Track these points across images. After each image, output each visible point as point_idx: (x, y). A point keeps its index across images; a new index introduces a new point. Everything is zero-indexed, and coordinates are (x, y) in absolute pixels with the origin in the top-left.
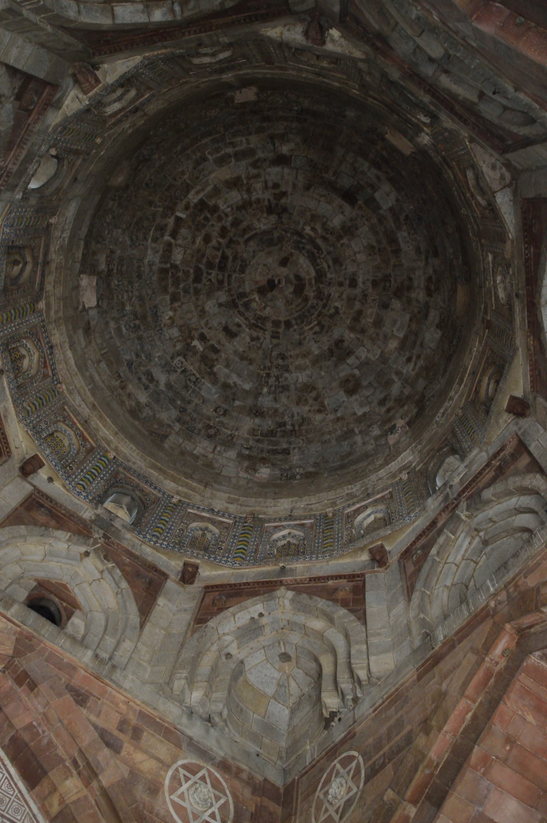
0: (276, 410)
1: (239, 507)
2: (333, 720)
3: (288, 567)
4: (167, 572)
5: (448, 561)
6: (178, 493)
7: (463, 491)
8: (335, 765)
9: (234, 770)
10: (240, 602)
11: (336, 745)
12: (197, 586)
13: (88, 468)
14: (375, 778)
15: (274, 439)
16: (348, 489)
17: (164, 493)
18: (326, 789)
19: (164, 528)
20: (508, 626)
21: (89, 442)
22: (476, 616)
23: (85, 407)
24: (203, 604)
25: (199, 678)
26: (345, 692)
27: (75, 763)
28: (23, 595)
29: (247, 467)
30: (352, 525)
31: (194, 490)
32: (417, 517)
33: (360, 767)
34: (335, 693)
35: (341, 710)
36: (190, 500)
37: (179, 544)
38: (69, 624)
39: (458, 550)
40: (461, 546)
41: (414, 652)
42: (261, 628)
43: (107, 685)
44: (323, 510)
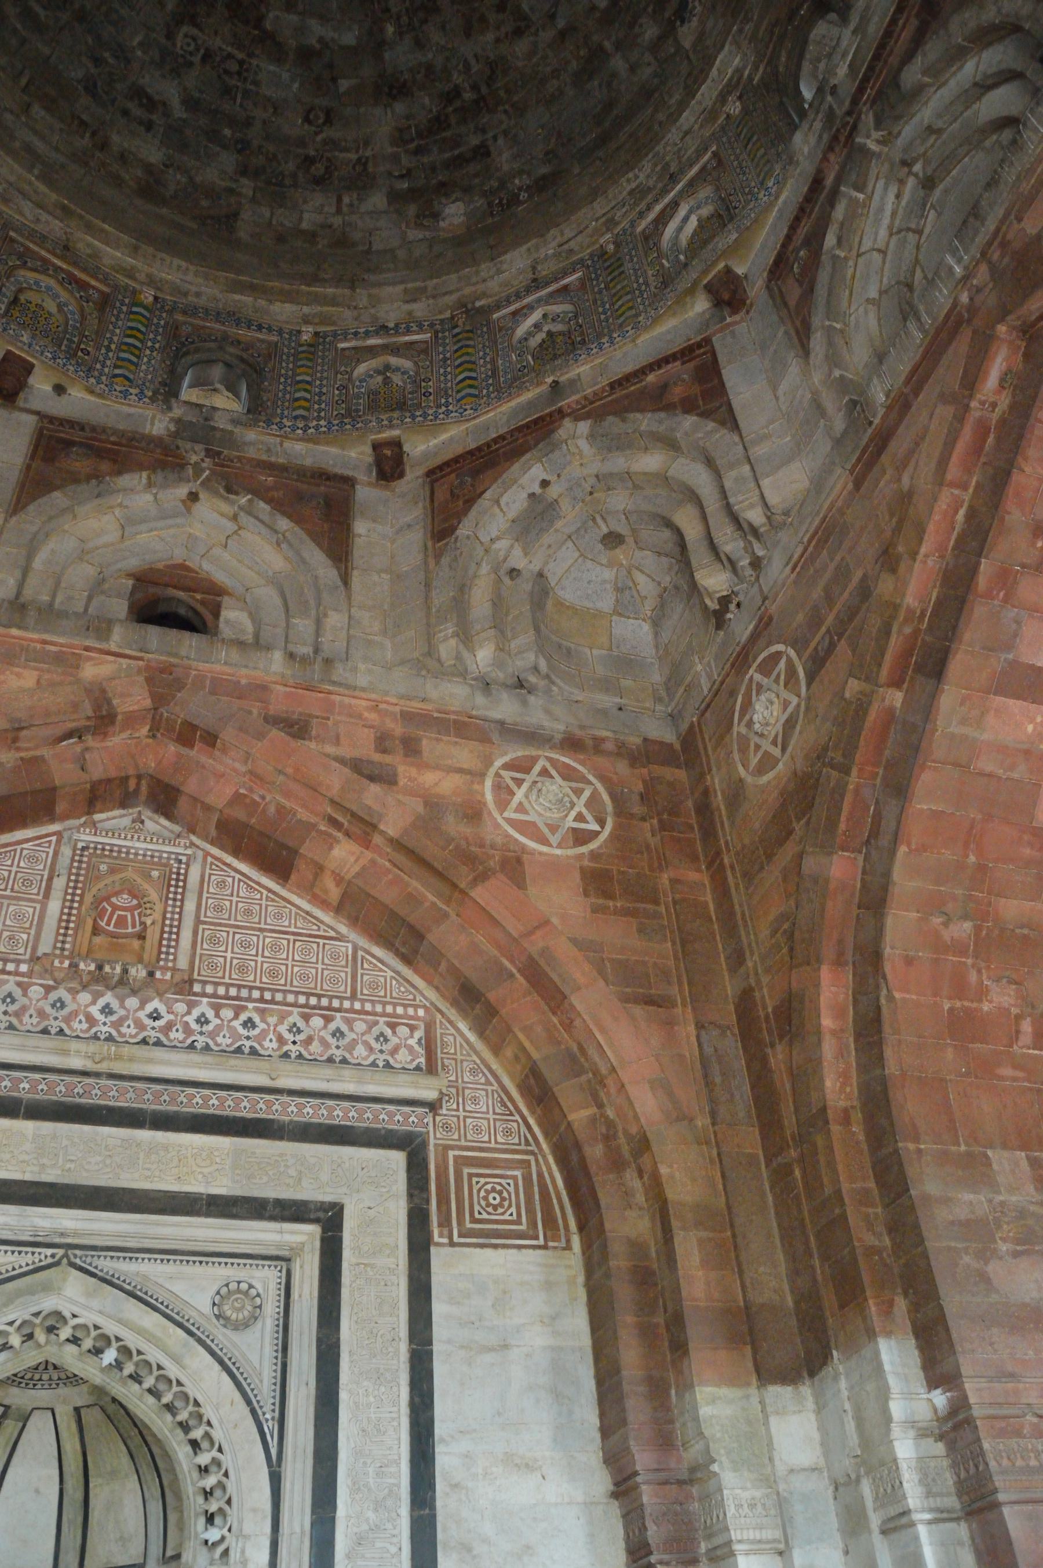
0: (429, 68)
1: (431, 301)
2: (727, 611)
3: (562, 379)
4: (350, 473)
5: (862, 250)
6: (306, 320)
7: (861, 90)
9: (589, 743)
10: (500, 475)
11: (743, 648)
12: (413, 477)
13: (115, 339)
15: (447, 134)
16: (628, 181)
17: (280, 332)
18: (747, 717)
19: (308, 396)
20: (1002, 329)
21: (94, 288)
22: (938, 331)
23: (50, 218)
24: (436, 504)
25: (478, 627)
26: (733, 557)
27: (333, 822)
28: (120, 608)
29: (418, 216)
30: (659, 250)
31: (333, 302)
32: (780, 184)
34: (719, 566)
36: (334, 324)
37: (349, 416)
38: (222, 625)
39: (878, 221)
40: (881, 210)
41: (838, 442)
42: (554, 505)
43: (330, 693)
44: (594, 243)
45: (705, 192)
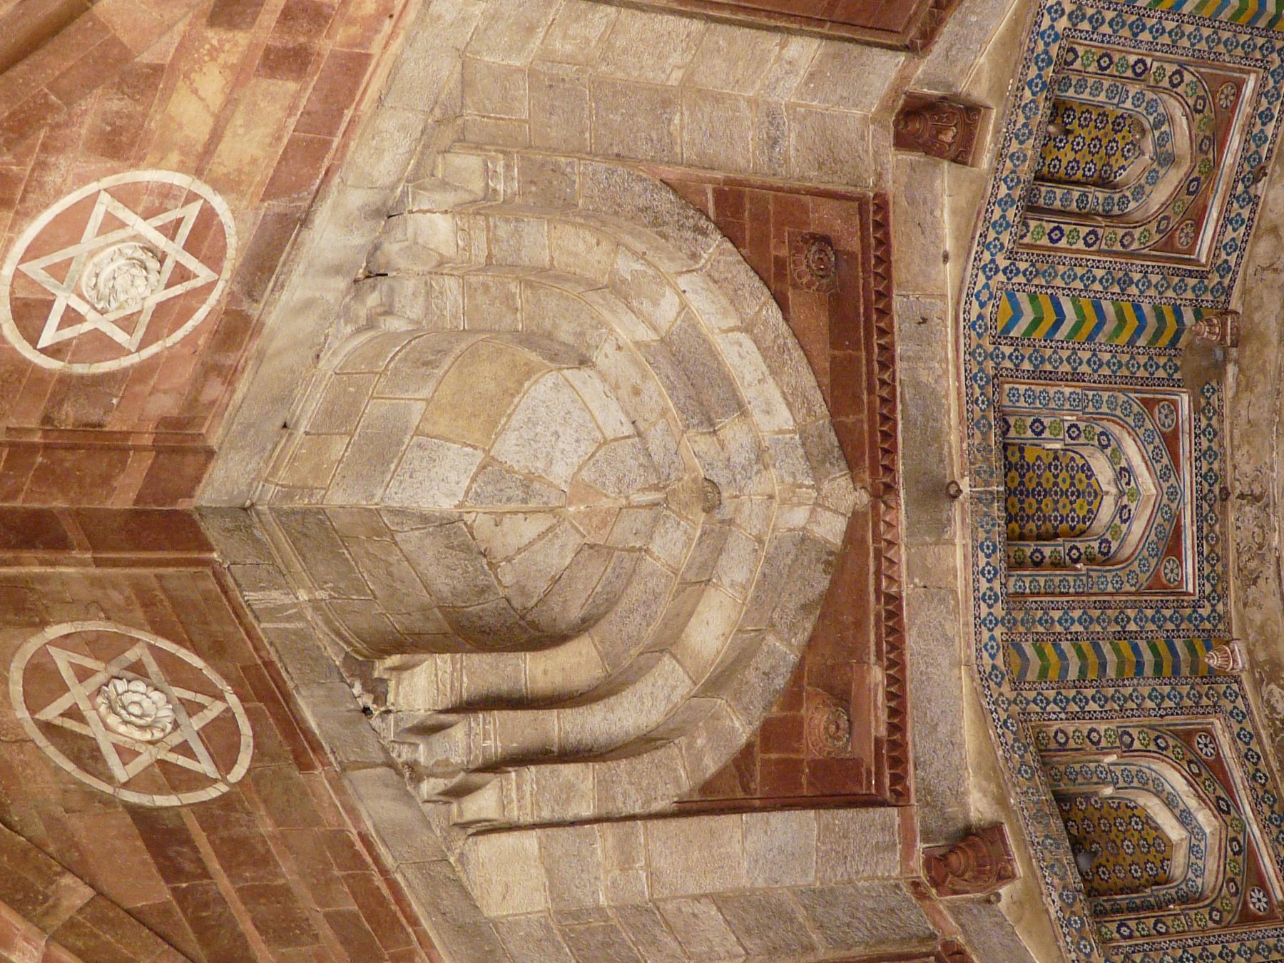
2: (368, 688)
3: (956, 511)
4: (938, 48)
8: (220, 697)
9: (230, 359)
14: (139, 843)
25: (503, 230)
33: (189, 789)
35: (391, 717)
44: (1243, 630)
45: (1210, 873)
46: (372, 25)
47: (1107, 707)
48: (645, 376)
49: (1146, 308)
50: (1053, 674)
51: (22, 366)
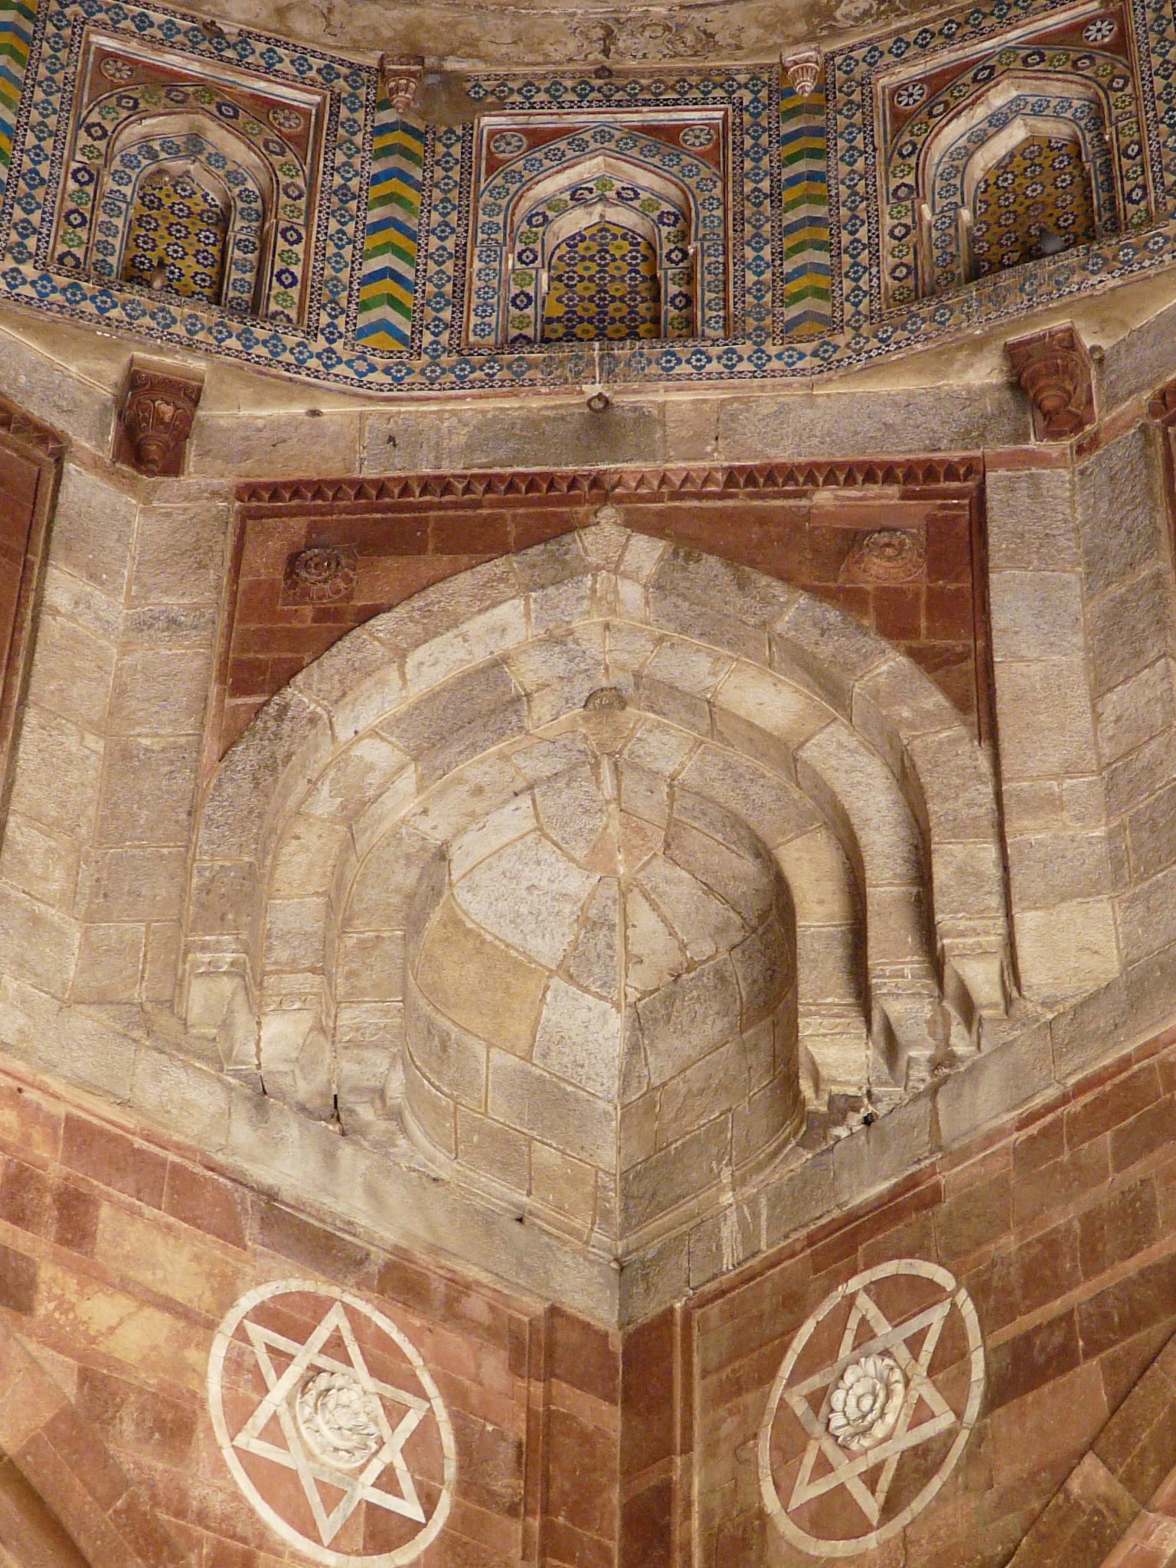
2: (841, 1121)
4: (58, 422)
8: (850, 1300)
9: (439, 1288)
14: (1030, 1398)
24: (244, 581)
25: (281, 953)
26: (901, 1035)
33: (964, 1337)
35: (875, 1090)
45: (1066, 89)
46: (31, 1114)
47: (864, 216)
48: (459, 781)
49: (376, 168)
50: (823, 282)
51: (448, 1542)
